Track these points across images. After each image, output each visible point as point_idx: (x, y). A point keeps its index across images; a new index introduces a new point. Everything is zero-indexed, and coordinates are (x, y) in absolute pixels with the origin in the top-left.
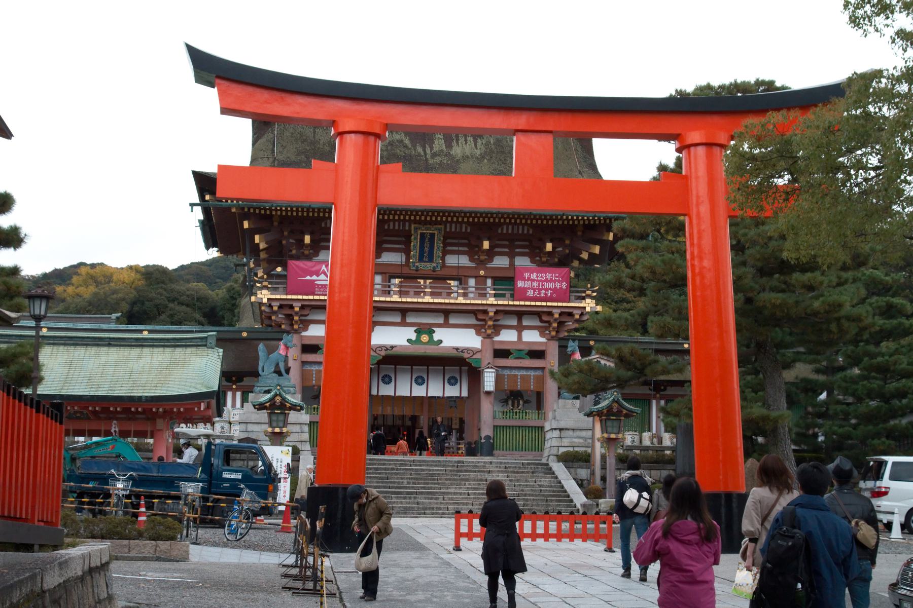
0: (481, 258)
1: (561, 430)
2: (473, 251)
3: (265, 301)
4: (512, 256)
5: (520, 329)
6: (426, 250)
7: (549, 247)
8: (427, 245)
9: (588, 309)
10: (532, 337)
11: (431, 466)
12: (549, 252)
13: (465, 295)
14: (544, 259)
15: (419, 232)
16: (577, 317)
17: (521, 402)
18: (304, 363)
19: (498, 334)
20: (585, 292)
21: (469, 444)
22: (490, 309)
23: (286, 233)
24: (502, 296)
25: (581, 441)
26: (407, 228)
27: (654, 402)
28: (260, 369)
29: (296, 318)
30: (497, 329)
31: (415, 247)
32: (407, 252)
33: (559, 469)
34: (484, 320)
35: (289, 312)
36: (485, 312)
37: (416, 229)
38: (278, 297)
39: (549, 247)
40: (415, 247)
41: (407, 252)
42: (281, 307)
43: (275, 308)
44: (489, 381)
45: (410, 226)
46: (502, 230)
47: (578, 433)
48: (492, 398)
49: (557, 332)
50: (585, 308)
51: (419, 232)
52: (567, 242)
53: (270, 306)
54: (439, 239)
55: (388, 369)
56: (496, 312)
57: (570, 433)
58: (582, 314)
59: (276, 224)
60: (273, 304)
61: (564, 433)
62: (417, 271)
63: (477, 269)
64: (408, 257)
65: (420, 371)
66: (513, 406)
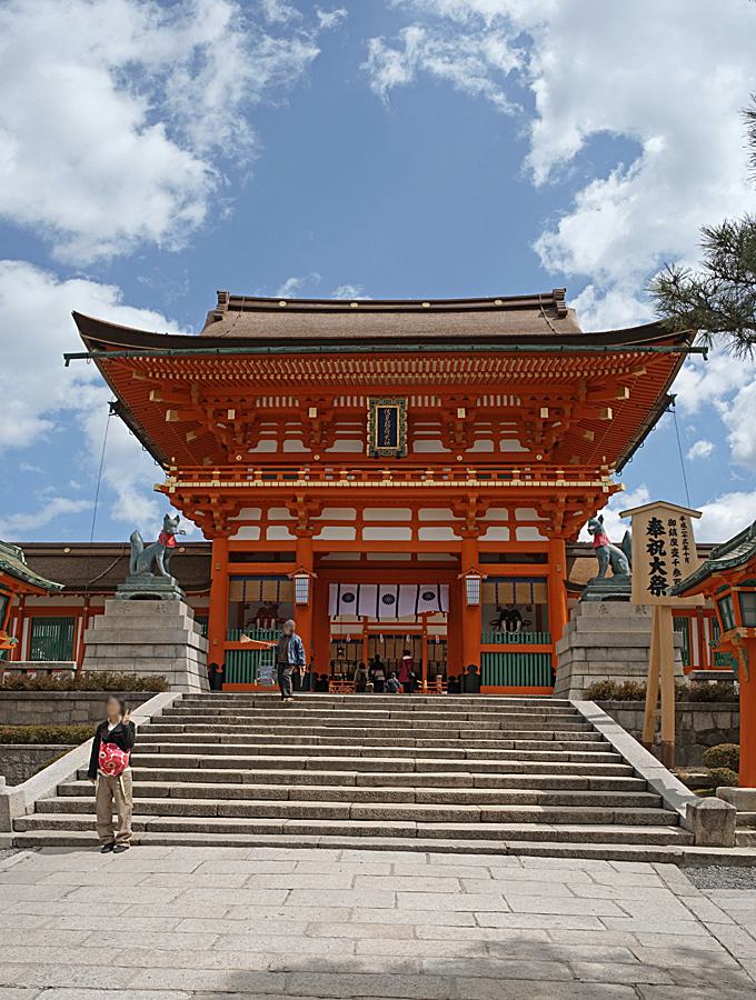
0: (455, 436)
1: (586, 648)
2: (447, 432)
3: (172, 490)
4: (496, 439)
5: (512, 524)
6: (387, 431)
7: (544, 413)
8: (387, 425)
9: (606, 490)
10: (528, 535)
11: (369, 708)
12: (546, 422)
13: (437, 477)
14: (538, 439)
15: (377, 407)
16: (591, 500)
17: (519, 624)
18: (232, 577)
19: (484, 534)
20: (598, 469)
21: (452, 678)
22: (469, 494)
23: (210, 414)
24: (488, 477)
25: (620, 665)
26: (362, 405)
27: (694, 620)
28: (131, 566)
29: (216, 515)
30: (482, 527)
31: (372, 427)
32: (363, 438)
33: (589, 709)
34: (464, 514)
35: (206, 508)
36: (465, 500)
37: (372, 403)
38: (189, 485)
39: (544, 413)
40: (372, 427)
41: (363, 438)
42: (196, 501)
43: (186, 501)
44: (473, 591)
45: (365, 401)
46: (482, 402)
47: (616, 654)
48: (477, 615)
49: (563, 527)
50: (601, 488)
51: (377, 407)
52: (568, 412)
53: (181, 499)
54: (402, 416)
55: (347, 588)
56: (479, 501)
57: (603, 652)
58: (596, 498)
59: (195, 400)
60: (183, 495)
61: (590, 652)
62: (376, 457)
63: (454, 454)
64: (366, 443)
65: (387, 589)
66: (508, 628)
